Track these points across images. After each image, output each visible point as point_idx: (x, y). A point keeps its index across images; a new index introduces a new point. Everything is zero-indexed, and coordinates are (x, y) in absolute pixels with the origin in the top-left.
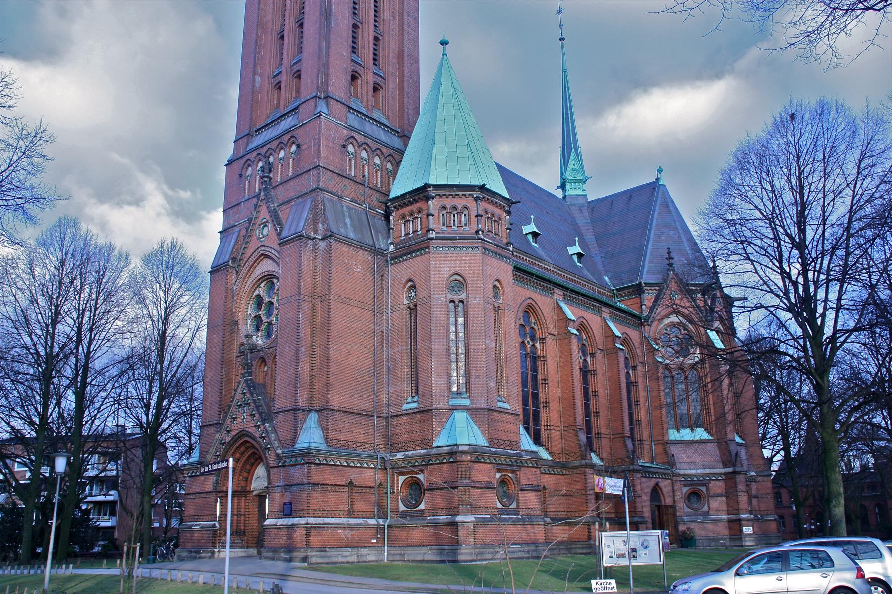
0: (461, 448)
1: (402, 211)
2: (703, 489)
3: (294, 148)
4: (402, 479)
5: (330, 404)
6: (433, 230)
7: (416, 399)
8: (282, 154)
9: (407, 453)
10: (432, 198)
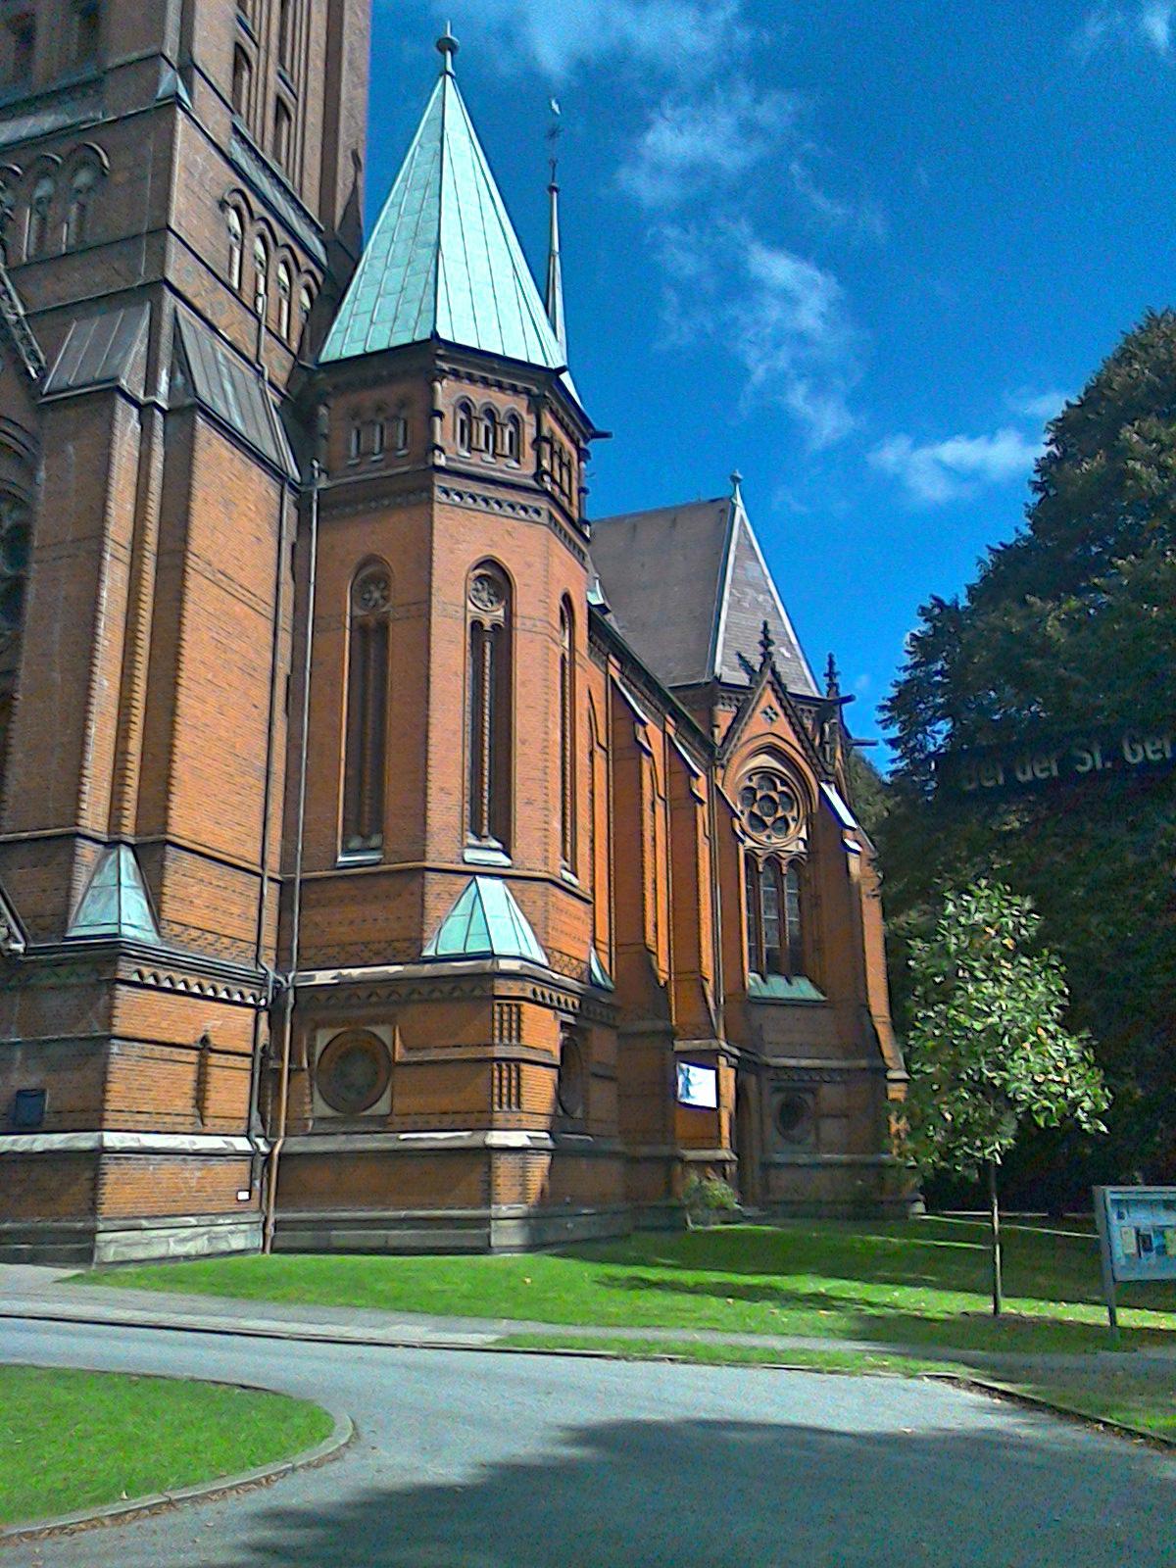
0: (505, 965)
1: (354, 399)
2: (809, 1098)
3: (84, 178)
4: (323, 1038)
5: (170, 829)
6: (442, 450)
7: (375, 841)
8: (45, 188)
9: (345, 972)
10: (443, 374)
